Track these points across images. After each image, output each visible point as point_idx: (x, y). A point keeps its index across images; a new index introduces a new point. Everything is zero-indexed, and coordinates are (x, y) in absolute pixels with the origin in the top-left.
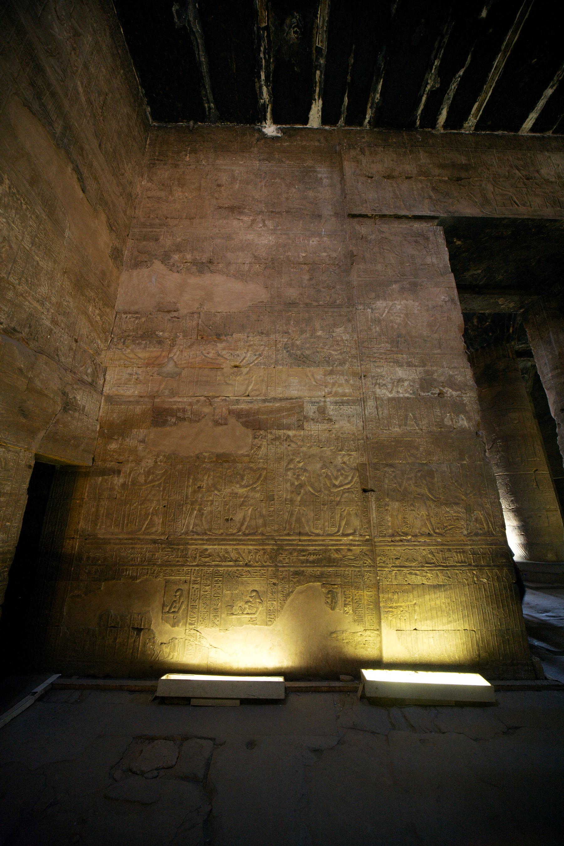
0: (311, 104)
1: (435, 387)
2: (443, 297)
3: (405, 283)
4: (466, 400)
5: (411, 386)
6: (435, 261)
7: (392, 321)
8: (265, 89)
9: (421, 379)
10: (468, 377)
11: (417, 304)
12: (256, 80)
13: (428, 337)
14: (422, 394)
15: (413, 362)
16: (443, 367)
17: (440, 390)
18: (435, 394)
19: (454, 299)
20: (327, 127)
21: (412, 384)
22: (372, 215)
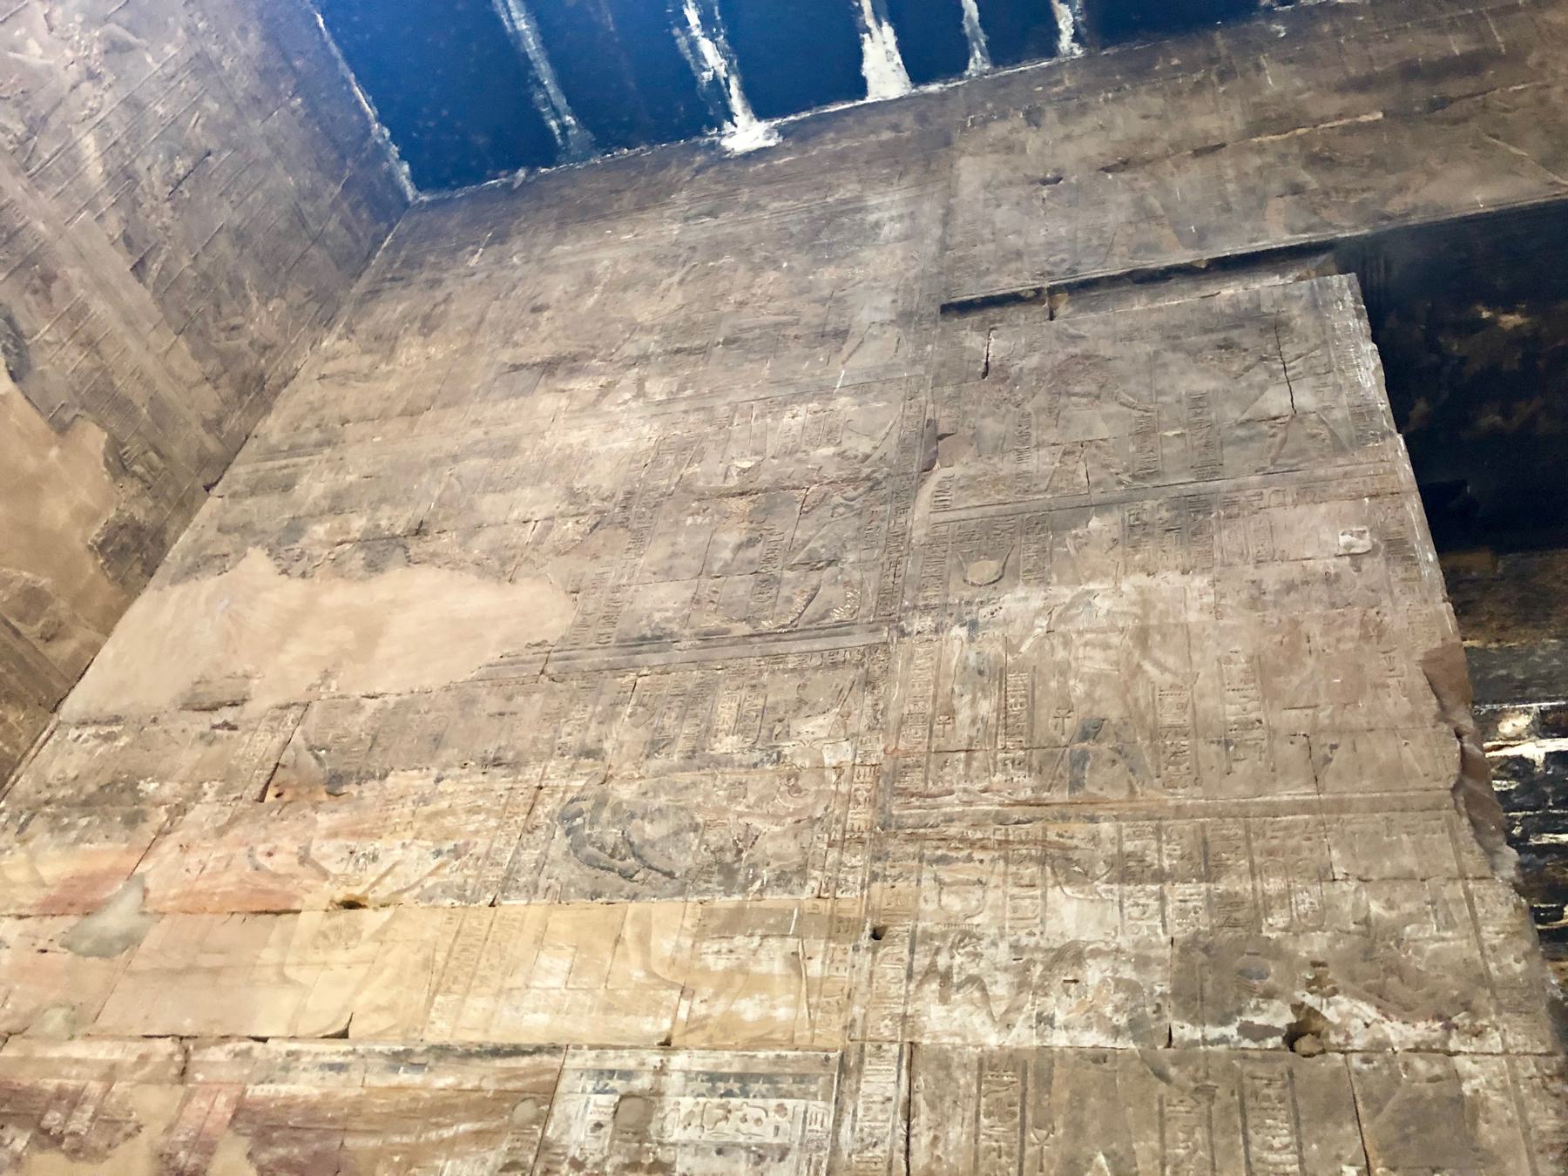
0: (860, 43)
1: (1269, 995)
2: (1343, 540)
3: (1148, 504)
4: (1478, 1071)
5: (1119, 983)
6: (1305, 399)
7: (1063, 670)
8: (706, 47)
9: (1186, 949)
10: (1491, 934)
11: (1200, 582)
12: (676, 31)
13: (1247, 726)
14: (1186, 1031)
15: (1152, 857)
16: (1324, 875)
17: (1297, 1008)
18: (1269, 1031)
19: (1403, 542)
20: (934, 88)
21: (1128, 973)
22: (1038, 291)
